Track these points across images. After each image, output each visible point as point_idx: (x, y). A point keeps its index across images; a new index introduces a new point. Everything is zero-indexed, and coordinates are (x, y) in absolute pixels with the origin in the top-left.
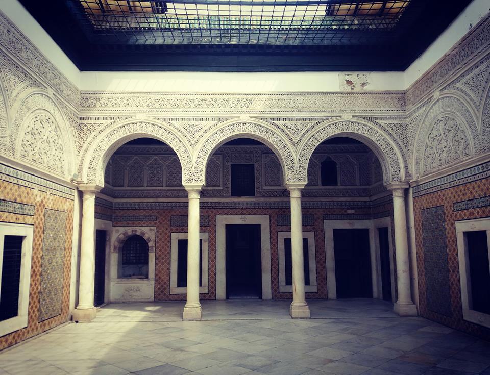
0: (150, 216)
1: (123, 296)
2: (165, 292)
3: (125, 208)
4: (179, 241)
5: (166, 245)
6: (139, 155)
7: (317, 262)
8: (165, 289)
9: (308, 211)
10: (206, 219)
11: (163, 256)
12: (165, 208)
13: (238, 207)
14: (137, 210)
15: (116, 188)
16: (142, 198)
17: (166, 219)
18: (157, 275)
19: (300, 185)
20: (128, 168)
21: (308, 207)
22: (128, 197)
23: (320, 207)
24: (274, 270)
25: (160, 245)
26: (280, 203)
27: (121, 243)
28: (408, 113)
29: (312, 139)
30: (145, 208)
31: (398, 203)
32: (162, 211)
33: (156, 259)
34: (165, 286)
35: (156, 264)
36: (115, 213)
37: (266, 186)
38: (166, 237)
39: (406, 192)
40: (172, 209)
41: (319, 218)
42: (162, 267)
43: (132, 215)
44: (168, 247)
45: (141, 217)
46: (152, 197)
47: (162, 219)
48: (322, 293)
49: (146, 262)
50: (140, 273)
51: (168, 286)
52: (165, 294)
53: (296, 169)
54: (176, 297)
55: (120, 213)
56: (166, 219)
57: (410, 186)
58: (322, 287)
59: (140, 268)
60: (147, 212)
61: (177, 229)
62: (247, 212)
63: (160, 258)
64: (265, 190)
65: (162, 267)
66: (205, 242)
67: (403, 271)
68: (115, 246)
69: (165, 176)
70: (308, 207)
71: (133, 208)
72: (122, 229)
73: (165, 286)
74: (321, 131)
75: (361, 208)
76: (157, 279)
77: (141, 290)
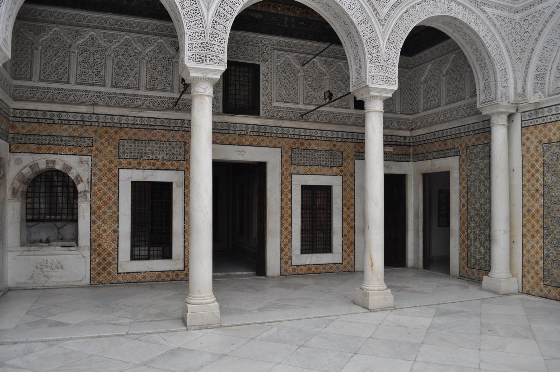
0: (81, 137)
1: (32, 277)
2: (110, 269)
3: (32, 120)
4: (133, 183)
5: (110, 189)
6: (62, 26)
7: (344, 220)
8: (109, 264)
9: (334, 146)
10: (181, 148)
11: (105, 208)
12: (108, 125)
13: (232, 132)
14: (57, 126)
15: (15, 82)
16: (67, 104)
17: (109, 144)
18: (95, 241)
19: (386, 91)
20: (40, 48)
21: (335, 139)
22: (39, 100)
23: (351, 140)
24: (285, 233)
25: (100, 189)
26: (297, 130)
27: (25, 184)
28: (520, 5)
29: (405, 17)
30: (71, 122)
31: (499, 134)
32: (100, 130)
33: (92, 213)
34: (110, 259)
35: (92, 222)
36: (13, 127)
37: (277, 101)
38: (110, 175)
39: (510, 116)
40: (121, 128)
41: (348, 157)
42: (104, 227)
43: (46, 133)
44: (114, 194)
45: (64, 138)
46: (83, 104)
47: (102, 144)
48: (348, 263)
49: (73, 218)
50: (60, 237)
51: (114, 259)
52: (109, 273)
53: (383, 63)
54: (129, 278)
55: (23, 128)
56: (109, 144)
57: (517, 110)
58: (349, 255)
59: (59, 228)
60: (74, 130)
61: (129, 163)
62: (247, 140)
63: (100, 213)
64: (275, 107)
65: (104, 227)
66: (178, 186)
67: (504, 231)
68: (14, 189)
69: (109, 69)
70: (335, 139)
71: (48, 121)
72: (27, 159)
73: (110, 259)
74: (417, 7)
75: (401, 145)
76: (95, 247)
77: (64, 268)
